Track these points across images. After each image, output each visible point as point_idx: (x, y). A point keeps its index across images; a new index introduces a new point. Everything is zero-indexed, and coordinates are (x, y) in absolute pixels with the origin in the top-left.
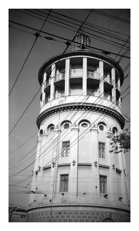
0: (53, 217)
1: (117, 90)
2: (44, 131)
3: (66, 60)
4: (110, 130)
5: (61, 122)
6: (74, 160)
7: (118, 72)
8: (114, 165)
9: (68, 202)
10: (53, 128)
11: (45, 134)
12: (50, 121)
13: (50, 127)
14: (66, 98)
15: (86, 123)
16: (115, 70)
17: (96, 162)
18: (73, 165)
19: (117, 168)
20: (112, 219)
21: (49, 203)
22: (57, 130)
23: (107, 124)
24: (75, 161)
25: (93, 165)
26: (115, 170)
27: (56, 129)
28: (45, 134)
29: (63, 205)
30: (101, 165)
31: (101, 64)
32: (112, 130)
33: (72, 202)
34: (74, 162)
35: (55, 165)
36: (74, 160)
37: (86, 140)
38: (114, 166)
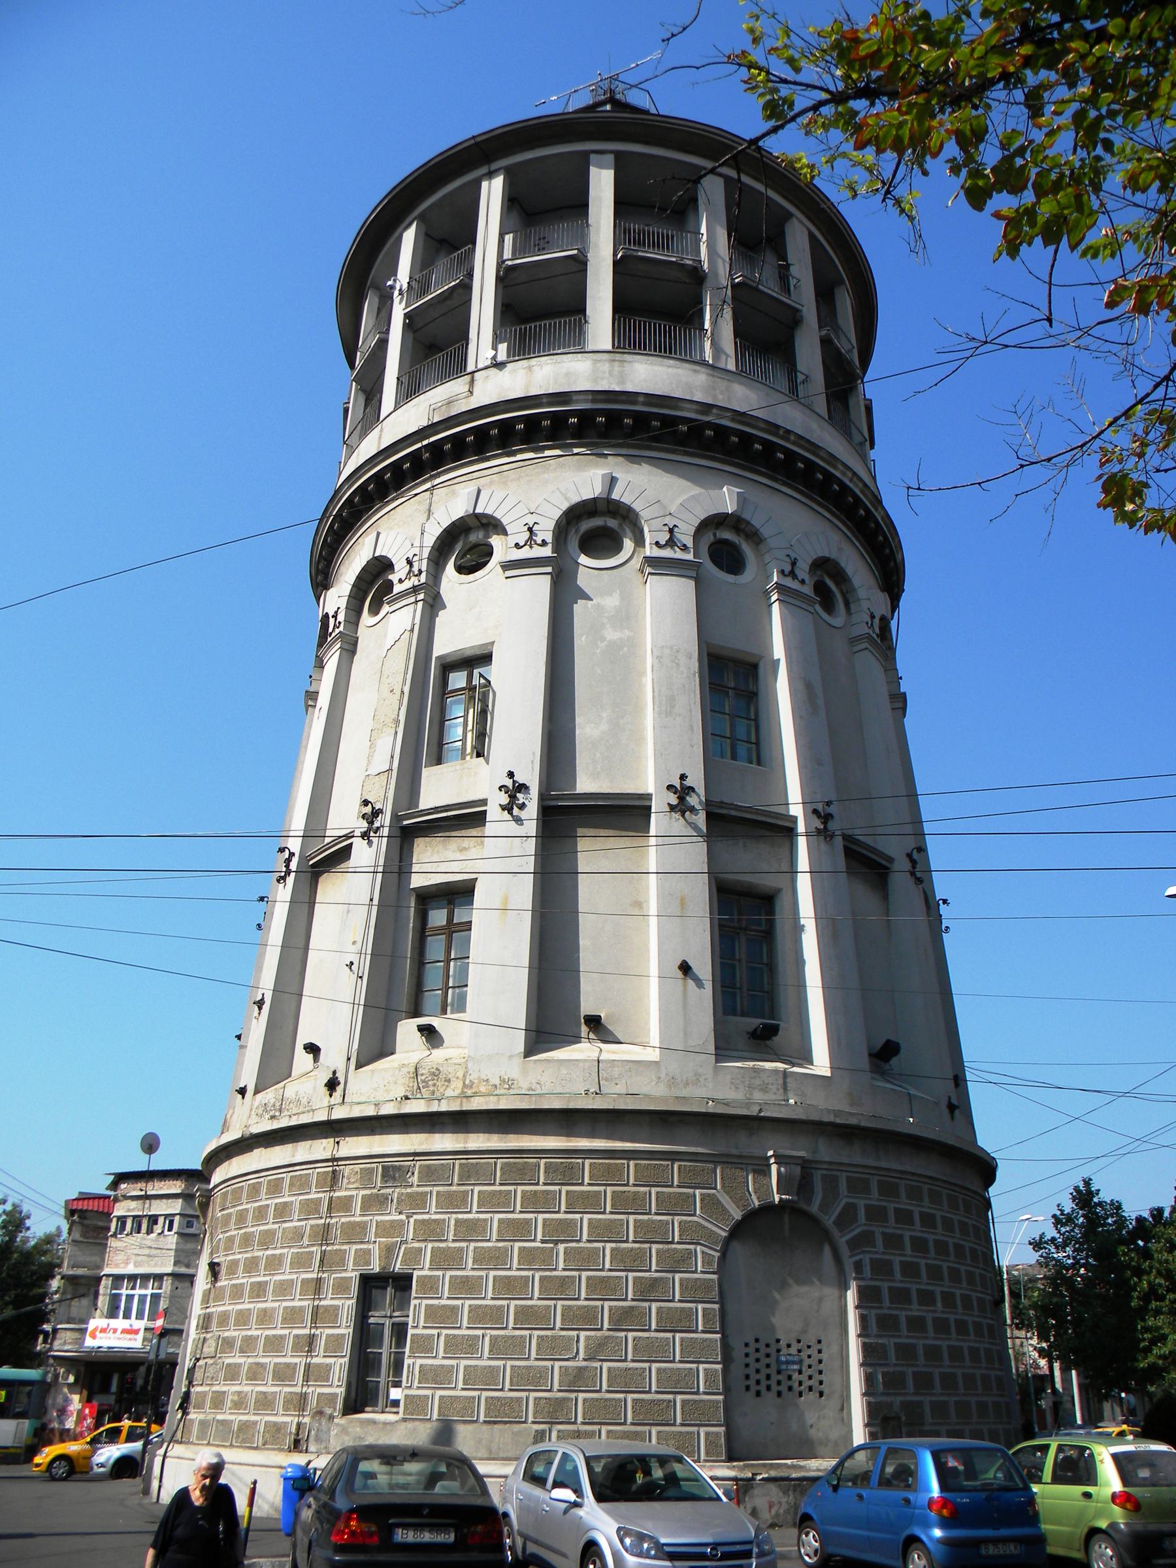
0: (345, 1205)
1: (826, 342)
2: (335, 616)
3: (485, 184)
4: (788, 569)
5: (434, 532)
6: (511, 775)
7: (834, 257)
8: (832, 809)
9: (455, 1089)
10: (389, 585)
11: (337, 631)
12: (369, 540)
13: (371, 583)
14: (472, 381)
15: (612, 523)
16: (812, 236)
17: (683, 777)
18: (503, 808)
19: (858, 833)
20: (814, 1208)
21: (321, 1098)
22: (407, 584)
23: (765, 532)
24: (520, 778)
25: (660, 803)
26: (839, 842)
27: (401, 581)
28: (337, 631)
29: (416, 1107)
30: (722, 804)
31: (712, 190)
32: (803, 570)
33: (483, 1089)
34: (516, 790)
35: (377, 824)
36: (511, 775)
37: (611, 635)
38: (826, 818)
